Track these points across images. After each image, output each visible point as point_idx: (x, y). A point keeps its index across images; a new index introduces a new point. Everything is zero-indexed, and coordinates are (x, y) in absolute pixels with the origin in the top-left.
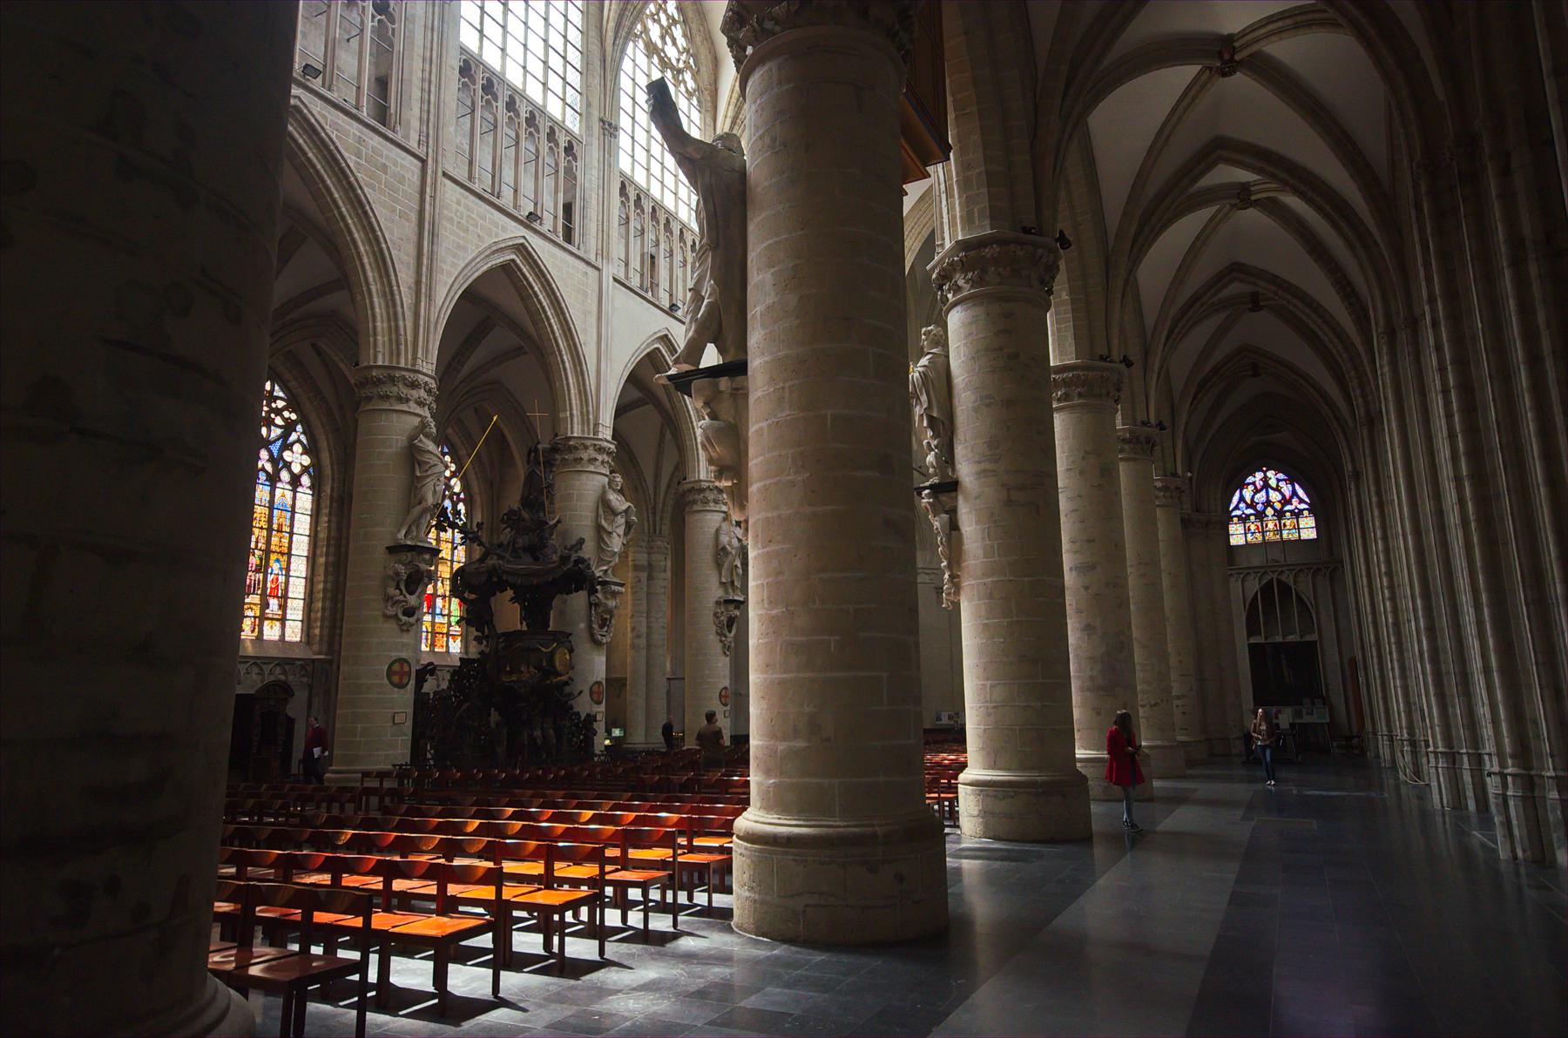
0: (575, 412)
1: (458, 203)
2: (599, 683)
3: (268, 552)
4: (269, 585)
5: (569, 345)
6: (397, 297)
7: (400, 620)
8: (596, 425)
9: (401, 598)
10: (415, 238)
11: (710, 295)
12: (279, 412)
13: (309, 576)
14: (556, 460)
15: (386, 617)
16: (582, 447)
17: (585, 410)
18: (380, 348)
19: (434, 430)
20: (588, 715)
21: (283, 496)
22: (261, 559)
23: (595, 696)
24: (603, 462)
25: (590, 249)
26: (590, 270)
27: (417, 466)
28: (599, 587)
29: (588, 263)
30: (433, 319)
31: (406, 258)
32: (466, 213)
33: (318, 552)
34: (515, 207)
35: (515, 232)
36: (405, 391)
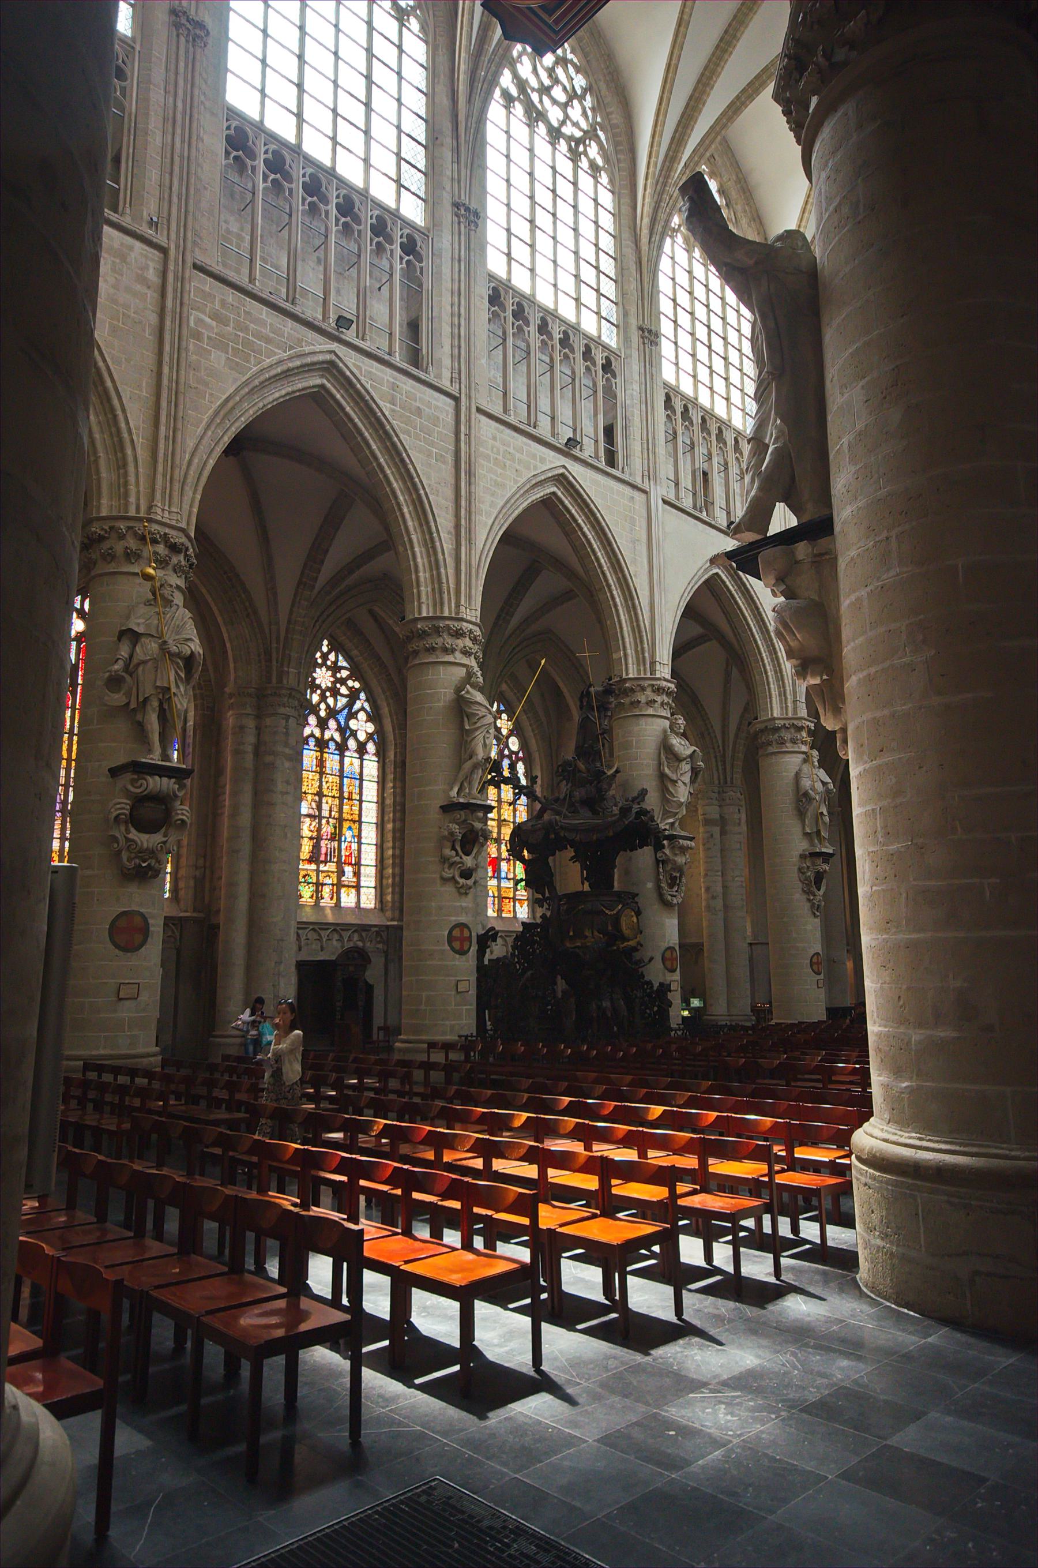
0: (629, 651)
1: (494, 438)
2: (671, 949)
3: (340, 820)
4: (343, 853)
5: (618, 579)
6: (438, 544)
7: (458, 883)
8: (653, 663)
9: (457, 859)
10: (452, 481)
11: (777, 439)
12: (343, 681)
14: (611, 703)
15: (445, 880)
18: (424, 599)
19: (481, 680)
20: (661, 984)
21: (351, 764)
22: (335, 828)
23: (668, 964)
24: (662, 704)
25: (635, 471)
26: (637, 494)
27: (466, 719)
28: (665, 842)
29: (634, 487)
30: (474, 563)
31: (444, 502)
32: (502, 448)
33: (386, 818)
34: (553, 435)
35: (554, 461)
36: (449, 641)
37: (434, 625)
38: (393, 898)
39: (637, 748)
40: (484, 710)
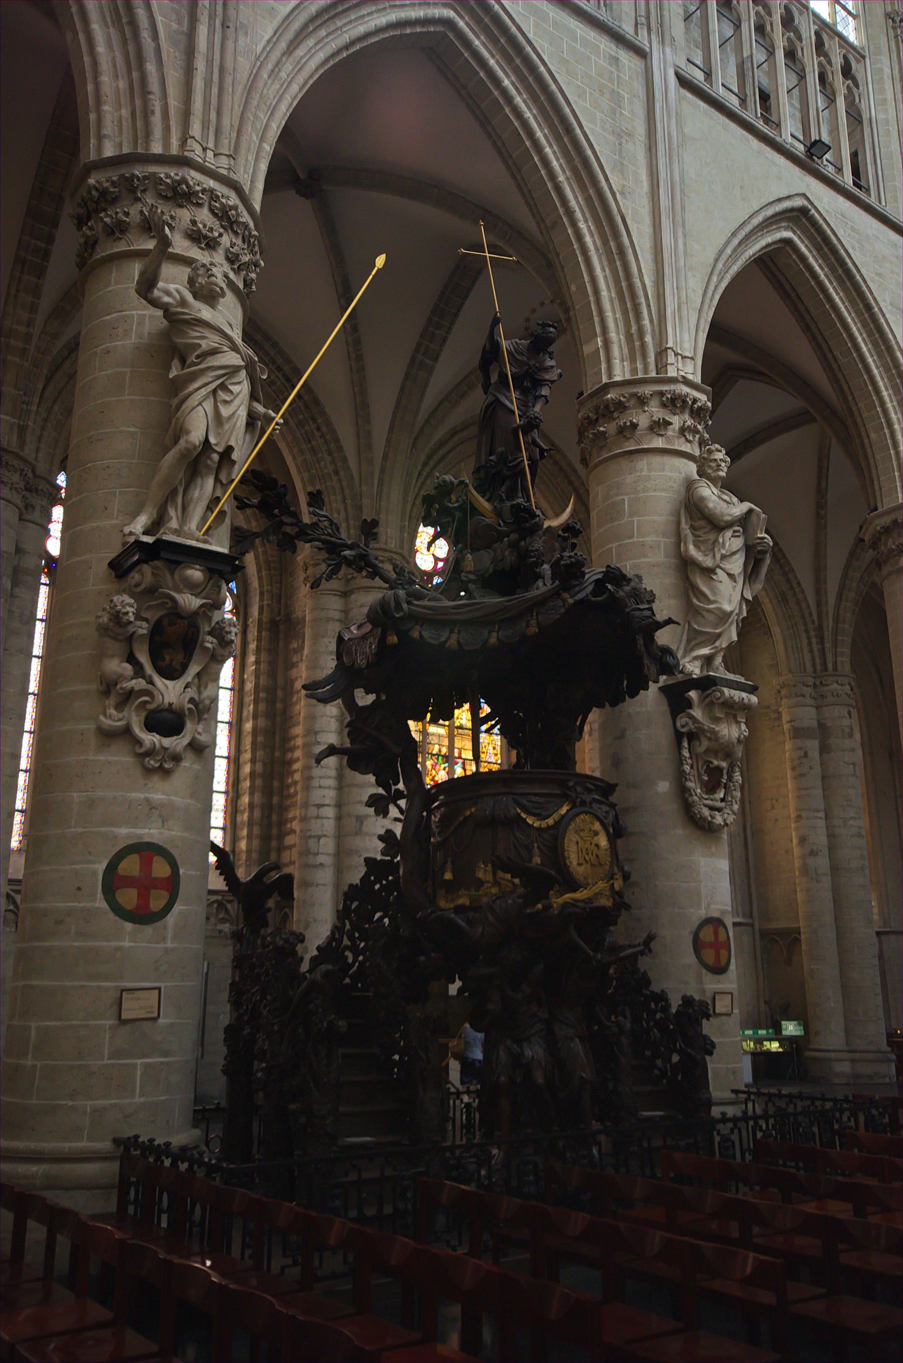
0: (613, 335)
2: (716, 923)
5: (588, 200)
7: (139, 742)
8: (662, 353)
9: (139, 684)
13: (232, 756)
14: (548, 369)
15: (108, 736)
16: (632, 402)
17: (634, 329)
23: (709, 955)
24: (683, 431)
26: (625, 56)
28: (693, 694)
29: (618, 38)
33: (245, 713)
37: (122, 176)
38: (249, 844)
39: (632, 515)
40: (217, 338)
